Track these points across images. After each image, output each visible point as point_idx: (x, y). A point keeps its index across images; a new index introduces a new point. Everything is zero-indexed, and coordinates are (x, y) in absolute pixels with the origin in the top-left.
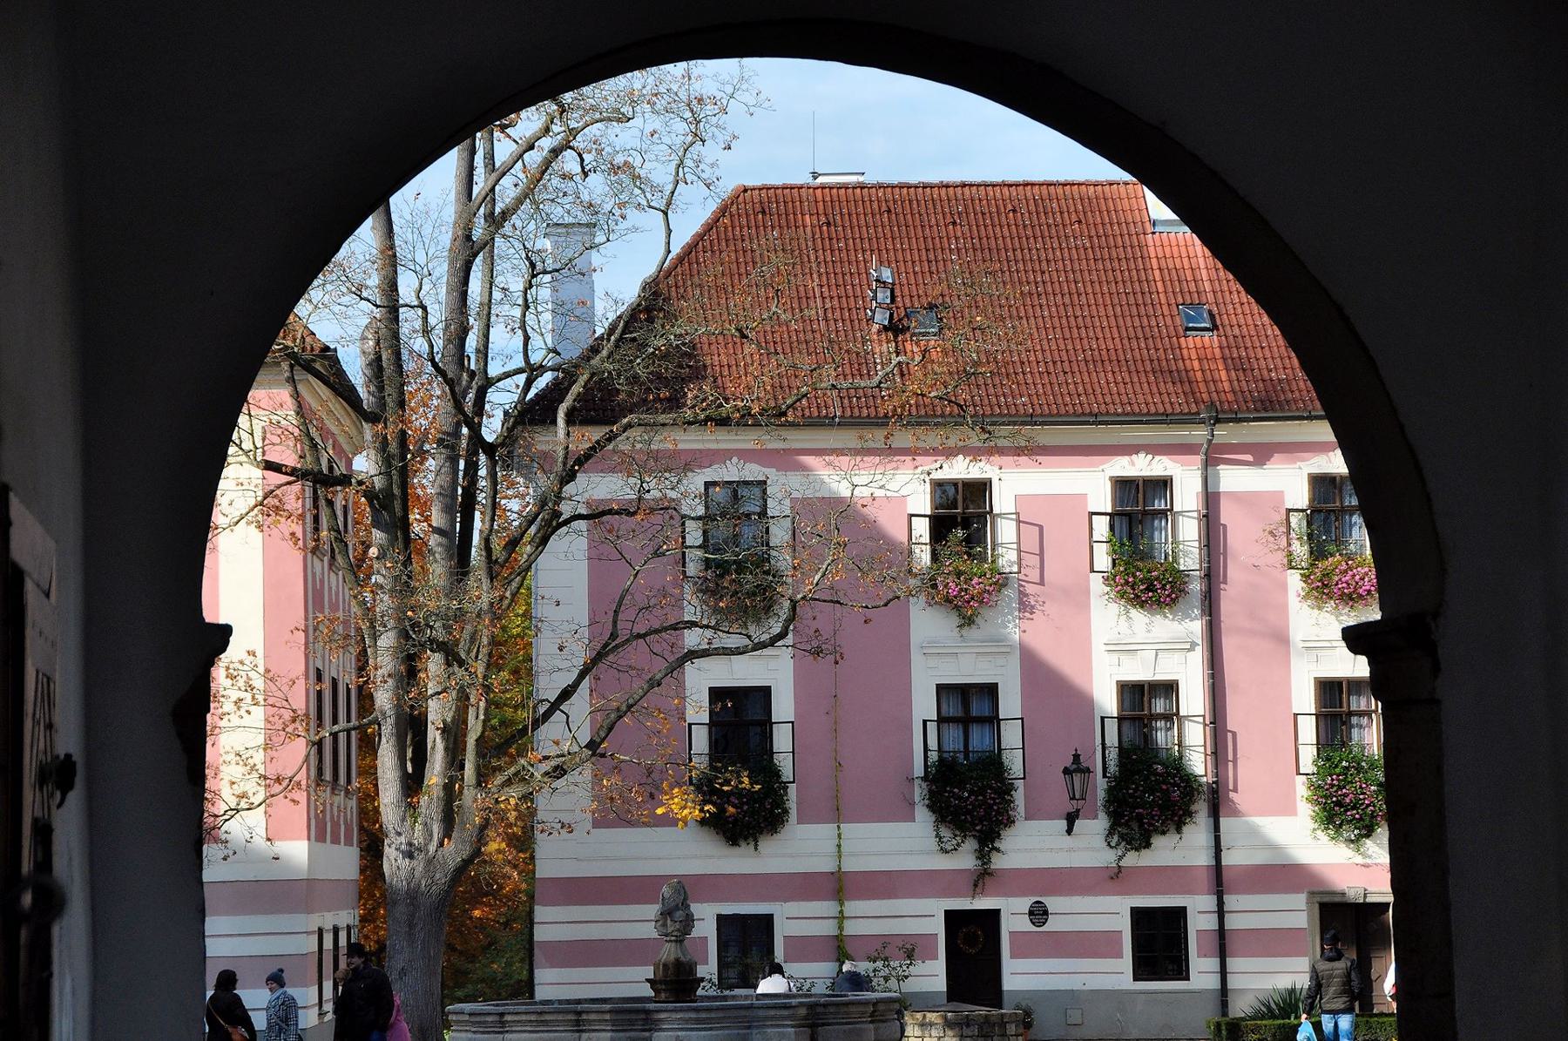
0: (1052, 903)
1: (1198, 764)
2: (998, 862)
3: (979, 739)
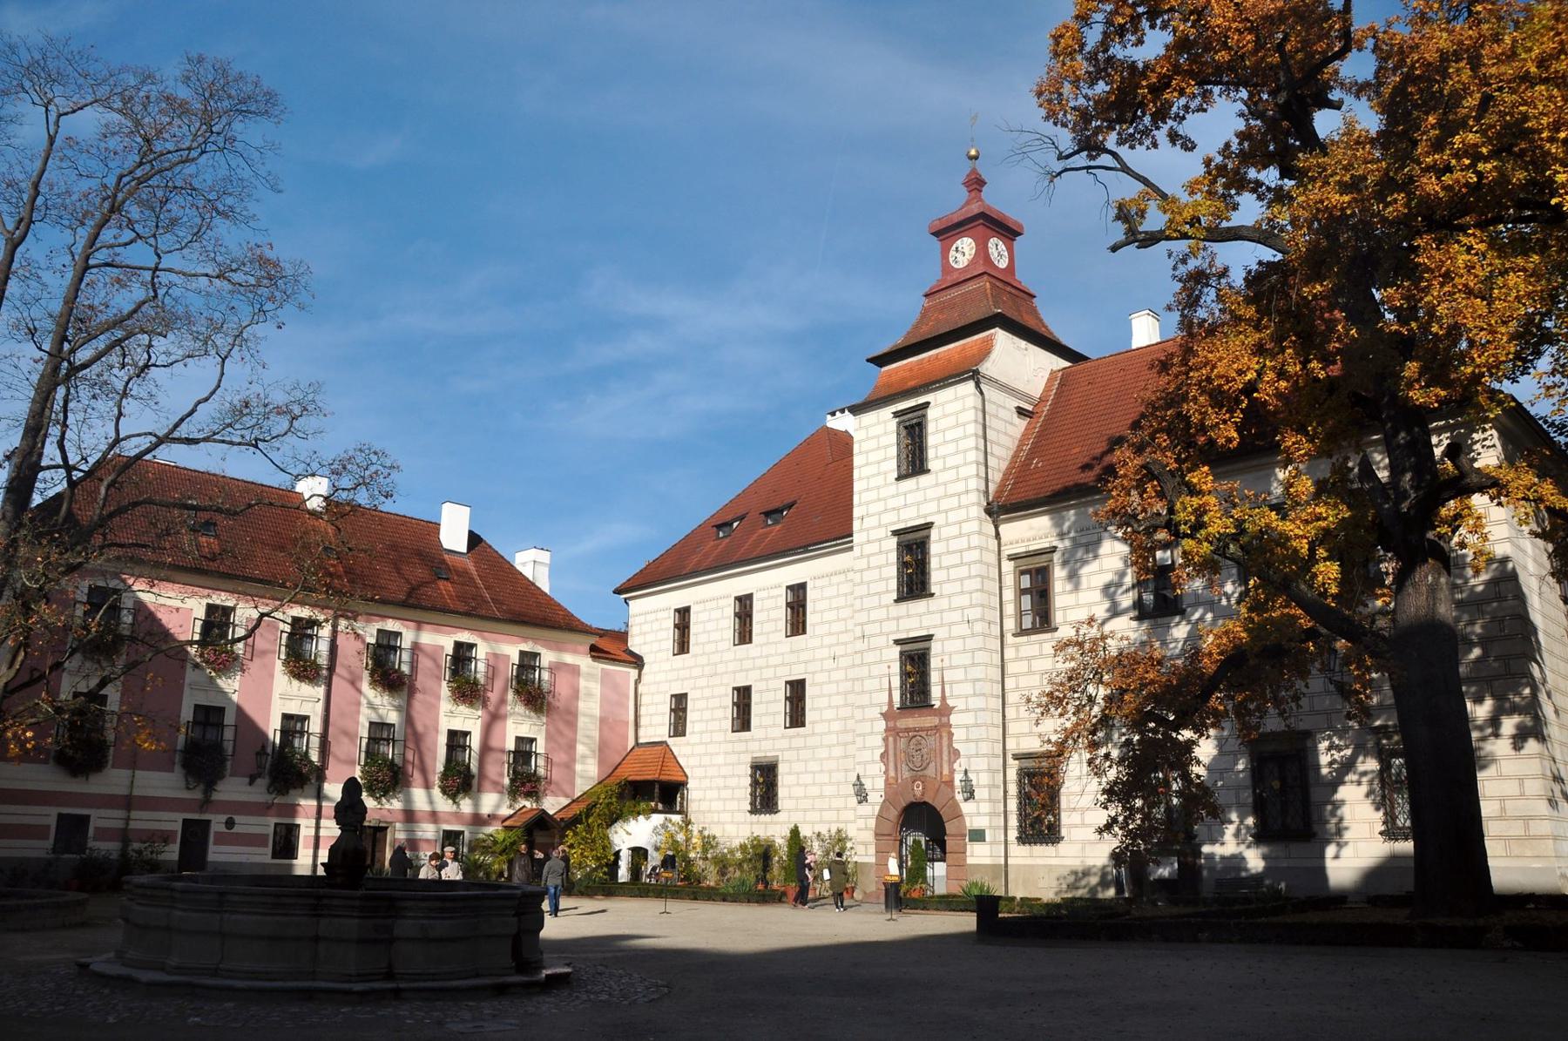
0: (237, 819)
1: (314, 757)
2: (216, 796)
3: (211, 734)
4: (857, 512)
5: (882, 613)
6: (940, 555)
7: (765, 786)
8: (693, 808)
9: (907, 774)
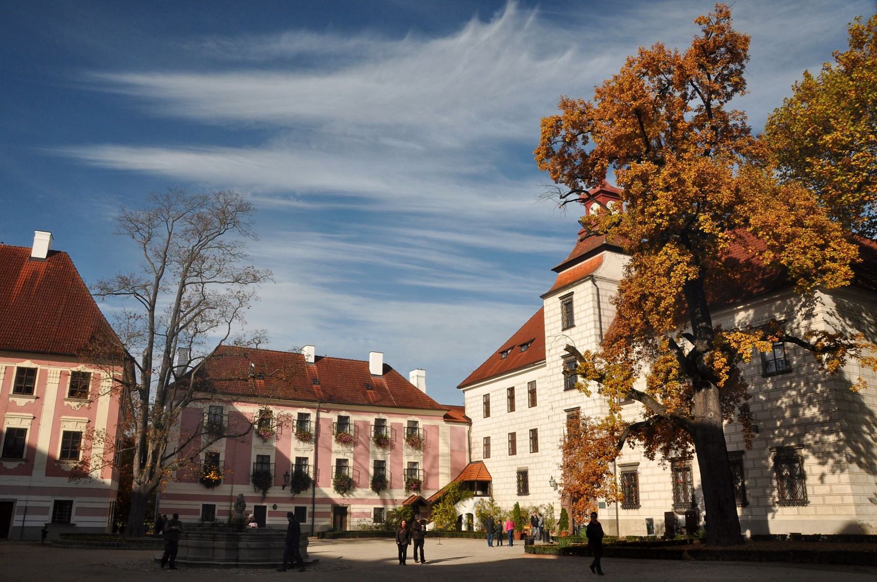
0: (278, 505)
1: (311, 476)
2: (268, 495)
3: (265, 467)
8: (494, 493)
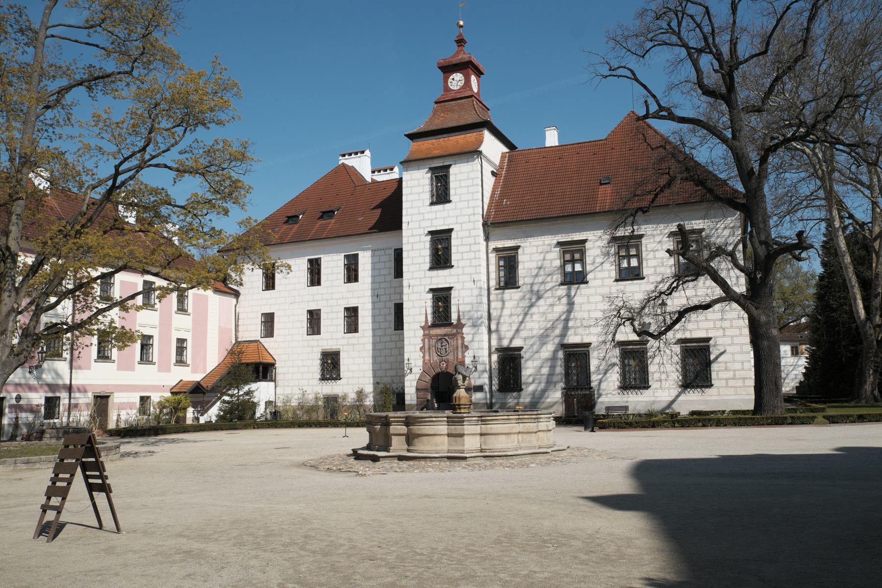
4: (404, 219)
5: (422, 274)
6: (457, 246)
7: (330, 364)
9: (436, 358)
